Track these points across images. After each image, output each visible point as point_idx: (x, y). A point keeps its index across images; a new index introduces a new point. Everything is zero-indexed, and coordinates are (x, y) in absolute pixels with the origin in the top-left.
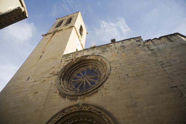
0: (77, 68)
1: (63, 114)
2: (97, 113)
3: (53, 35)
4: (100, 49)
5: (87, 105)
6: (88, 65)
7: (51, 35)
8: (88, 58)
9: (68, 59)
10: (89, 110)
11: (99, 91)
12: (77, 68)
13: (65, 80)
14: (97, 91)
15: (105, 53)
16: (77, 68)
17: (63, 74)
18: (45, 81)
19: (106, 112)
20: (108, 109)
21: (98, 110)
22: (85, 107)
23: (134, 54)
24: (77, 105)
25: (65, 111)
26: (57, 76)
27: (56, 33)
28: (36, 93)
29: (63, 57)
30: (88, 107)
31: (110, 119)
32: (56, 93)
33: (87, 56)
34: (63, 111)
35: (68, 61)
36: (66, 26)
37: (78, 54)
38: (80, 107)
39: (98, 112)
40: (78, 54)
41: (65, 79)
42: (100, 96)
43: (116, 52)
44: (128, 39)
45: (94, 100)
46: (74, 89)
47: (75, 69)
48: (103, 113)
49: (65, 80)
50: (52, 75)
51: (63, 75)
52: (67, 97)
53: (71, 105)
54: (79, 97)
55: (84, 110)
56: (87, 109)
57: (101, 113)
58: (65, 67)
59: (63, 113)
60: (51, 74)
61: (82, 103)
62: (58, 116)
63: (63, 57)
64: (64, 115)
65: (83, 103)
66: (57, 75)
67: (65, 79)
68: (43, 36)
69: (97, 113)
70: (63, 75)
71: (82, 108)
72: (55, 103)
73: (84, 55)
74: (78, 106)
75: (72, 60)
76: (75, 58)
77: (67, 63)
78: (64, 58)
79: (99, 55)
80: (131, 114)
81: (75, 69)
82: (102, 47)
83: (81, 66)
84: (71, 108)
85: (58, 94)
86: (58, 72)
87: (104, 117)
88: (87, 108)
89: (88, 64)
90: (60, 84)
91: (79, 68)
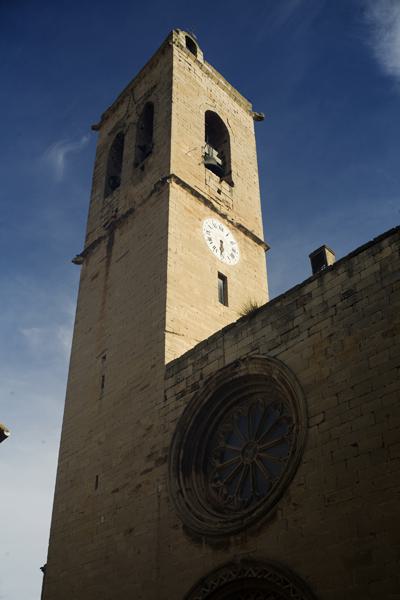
0: (219, 415)
1: (204, 592)
2: (279, 584)
3: (110, 247)
4: (272, 318)
6: (252, 395)
7: (104, 244)
8: (242, 370)
9: (182, 386)
11: (279, 512)
12: (221, 412)
13: (193, 473)
14: (274, 515)
15: (291, 343)
16: (219, 415)
17: (182, 452)
18: (140, 486)
23: (385, 335)
24: (230, 565)
26: (166, 465)
27: (117, 233)
28: (131, 531)
29: (166, 378)
32: (176, 527)
33: (236, 364)
34: (202, 582)
35: (183, 393)
36: (141, 179)
37: (206, 358)
39: (279, 581)
40: (210, 358)
41: (193, 467)
43: (325, 334)
44: (370, 245)
45: (268, 545)
46: (226, 496)
47: (216, 420)
49: (193, 473)
50: (151, 464)
51: (181, 457)
52: (203, 539)
54: (232, 539)
56: (255, 575)
57: (287, 584)
58: (181, 425)
60: (149, 456)
63: (166, 378)
66: (164, 460)
67: (193, 467)
68: (76, 262)
70: (181, 457)
71: (245, 571)
73: (227, 363)
75: (195, 387)
76: (201, 378)
77: (182, 404)
78: (171, 381)
79: (273, 353)
81: (216, 420)
82: (278, 304)
83: (229, 404)
85: (181, 531)
86: (165, 450)
88: (256, 571)
89: (251, 391)
90: (181, 491)
91: (226, 411)
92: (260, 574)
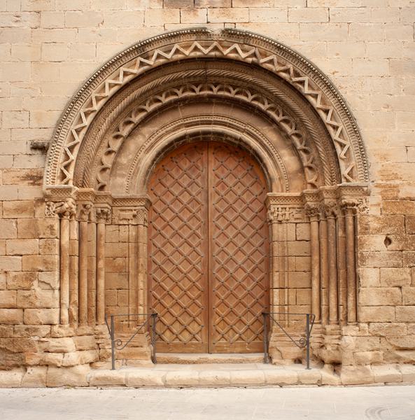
1: (142, 64)
5: (245, 37)
10: (250, 60)
19: (317, 74)
20: (324, 66)
21: (290, 66)
22: (236, 46)
24: (201, 33)
25: (148, 49)
30: (246, 46)
31: (332, 100)
34: (141, 49)
38: (215, 44)
39: (287, 71)
42: (299, 7)
48: (306, 79)
53: (172, 28)
55: (233, 55)
56: (243, 55)
59: (141, 56)
61: (222, 27)
62: (123, 69)
64: (146, 68)
65: (228, 26)
69: (283, 75)
72: (93, 8)
74: (203, 37)
80: (404, 95)
84: (173, 41)
87: (311, 92)
88: (244, 51)
92: (254, 55)
